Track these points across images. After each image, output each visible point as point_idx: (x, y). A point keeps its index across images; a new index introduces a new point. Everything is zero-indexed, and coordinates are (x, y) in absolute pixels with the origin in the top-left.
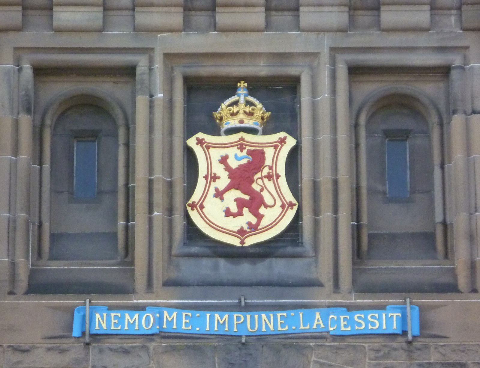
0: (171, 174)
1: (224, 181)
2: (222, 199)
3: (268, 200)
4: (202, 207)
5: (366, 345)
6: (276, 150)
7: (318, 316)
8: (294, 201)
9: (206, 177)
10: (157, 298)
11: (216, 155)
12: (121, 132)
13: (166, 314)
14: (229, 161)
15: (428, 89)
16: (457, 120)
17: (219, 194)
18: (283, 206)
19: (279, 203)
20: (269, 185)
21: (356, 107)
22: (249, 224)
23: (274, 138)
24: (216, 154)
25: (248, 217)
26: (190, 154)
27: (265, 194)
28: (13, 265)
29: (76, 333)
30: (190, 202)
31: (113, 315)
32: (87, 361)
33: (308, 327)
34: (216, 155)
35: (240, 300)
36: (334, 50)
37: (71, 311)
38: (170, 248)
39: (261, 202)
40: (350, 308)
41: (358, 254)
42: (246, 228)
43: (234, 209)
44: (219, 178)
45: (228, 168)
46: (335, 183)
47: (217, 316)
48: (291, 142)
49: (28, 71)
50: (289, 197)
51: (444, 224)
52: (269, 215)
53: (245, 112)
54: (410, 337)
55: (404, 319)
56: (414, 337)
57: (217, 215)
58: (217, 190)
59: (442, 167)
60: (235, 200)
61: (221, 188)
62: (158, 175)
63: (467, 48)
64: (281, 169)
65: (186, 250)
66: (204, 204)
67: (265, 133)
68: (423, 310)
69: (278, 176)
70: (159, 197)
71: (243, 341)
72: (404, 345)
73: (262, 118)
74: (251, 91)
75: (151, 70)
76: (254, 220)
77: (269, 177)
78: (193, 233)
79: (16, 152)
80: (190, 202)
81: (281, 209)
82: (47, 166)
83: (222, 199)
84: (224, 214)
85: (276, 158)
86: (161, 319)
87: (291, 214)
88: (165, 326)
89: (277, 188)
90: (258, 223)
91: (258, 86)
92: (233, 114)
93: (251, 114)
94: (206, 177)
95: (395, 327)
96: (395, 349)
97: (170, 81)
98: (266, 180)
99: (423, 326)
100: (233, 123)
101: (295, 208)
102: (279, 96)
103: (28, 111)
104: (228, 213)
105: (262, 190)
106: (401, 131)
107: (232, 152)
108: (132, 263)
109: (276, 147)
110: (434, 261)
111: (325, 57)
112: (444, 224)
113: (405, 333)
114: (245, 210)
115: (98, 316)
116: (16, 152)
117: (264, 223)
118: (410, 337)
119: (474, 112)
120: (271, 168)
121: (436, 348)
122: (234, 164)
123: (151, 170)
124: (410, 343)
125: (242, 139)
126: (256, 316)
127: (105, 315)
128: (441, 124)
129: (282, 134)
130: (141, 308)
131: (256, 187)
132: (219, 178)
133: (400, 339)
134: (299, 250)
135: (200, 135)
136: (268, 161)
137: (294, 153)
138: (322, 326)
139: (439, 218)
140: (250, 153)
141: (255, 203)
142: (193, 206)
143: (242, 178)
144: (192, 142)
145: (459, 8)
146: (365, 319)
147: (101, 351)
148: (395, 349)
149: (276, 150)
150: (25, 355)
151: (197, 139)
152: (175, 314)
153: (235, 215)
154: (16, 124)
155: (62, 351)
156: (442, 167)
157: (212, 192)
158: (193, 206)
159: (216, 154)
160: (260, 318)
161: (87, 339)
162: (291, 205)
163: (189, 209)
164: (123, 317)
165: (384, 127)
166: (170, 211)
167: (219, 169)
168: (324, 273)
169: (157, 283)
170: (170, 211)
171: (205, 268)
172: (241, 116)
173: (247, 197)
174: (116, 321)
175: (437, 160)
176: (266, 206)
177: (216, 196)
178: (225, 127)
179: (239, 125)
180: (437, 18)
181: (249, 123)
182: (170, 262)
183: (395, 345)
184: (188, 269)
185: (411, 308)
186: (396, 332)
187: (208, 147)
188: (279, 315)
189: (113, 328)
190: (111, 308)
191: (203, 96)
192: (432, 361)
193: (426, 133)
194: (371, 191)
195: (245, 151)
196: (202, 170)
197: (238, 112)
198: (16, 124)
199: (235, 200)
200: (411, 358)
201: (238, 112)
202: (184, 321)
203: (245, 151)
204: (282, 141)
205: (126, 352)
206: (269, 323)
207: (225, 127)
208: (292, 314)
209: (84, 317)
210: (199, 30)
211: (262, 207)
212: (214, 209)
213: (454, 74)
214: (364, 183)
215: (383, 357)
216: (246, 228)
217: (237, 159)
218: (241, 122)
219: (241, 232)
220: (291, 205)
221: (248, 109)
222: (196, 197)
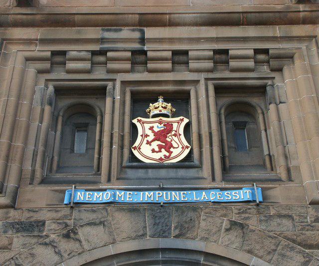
0: (123, 131)
1: (152, 137)
2: (150, 145)
3: (175, 145)
4: (140, 148)
5: (232, 207)
6: (179, 124)
7: (204, 193)
8: (189, 145)
9: (142, 136)
10: (113, 185)
11: (147, 127)
12: (99, 118)
13: (118, 193)
14: (154, 129)
15: (255, 101)
16: (272, 107)
17: (149, 143)
18: (183, 148)
19: (181, 146)
20: (176, 139)
21: (219, 108)
22: (165, 156)
23: (178, 119)
24: (147, 126)
25: (164, 152)
26: (134, 128)
27: (173, 143)
28: (33, 171)
29: (66, 202)
30: (134, 146)
31: (87, 193)
32: (71, 216)
33: (199, 199)
34: (147, 127)
35: (160, 186)
36: (207, 79)
37: (63, 192)
38: (122, 163)
39: (172, 146)
40: (222, 189)
41: (224, 169)
42: (163, 157)
43: (157, 149)
44: (149, 136)
45: (153, 132)
46: (210, 134)
47: (147, 193)
48: (186, 121)
49: (51, 88)
50: (186, 143)
51: (269, 155)
52: (175, 152)
53: (162, 107)
54: (258, 202)
55: (253, 194)
56: (260, 202)
57: (147, 152)
58: (148, 141)
59: (266, 131)
60: (157, 146)
61: (150, 140)
62: (116, 129)
63: (274, 78)
64: (181, 131)
65: (131, 164)
66: (141, 147)
67: (172, 117)
68: (263, 190)
69: (180, 135)
70: (116, 139)
71: (162, 204)
72: (255, 207)
73: (171, 110)
74: (165, 100)
75: (114, 88)
76: (167, 154)
77: (175, 135)
78: (133, 158)
79: (41, 122)
80: (134, 146)
81: (182, 149)
82: (59, 133)
83: (150, 145)
84: (151, 151)
85: (178, 127)
86: (114, 195)
87: (187, 151)
88: (117, 199)
89: (180, 140)
90: (170, 155)
91: (168, 97)
92: (156, 108)
93: (165, 108)
94: (142, 136)
95: (248, 197)
96: (250, 209)
97: (123, 94)
98: (173, 137)
99: (265, 198)
100: (157, 112)
101: (189, 149)
102: (180, 100)
103: (50, 104)
104: (153, 151)
105: (171, 141)
106: (242, 122)
107: (155, 125)
108: (100, 174)
109: (178, 123)
110: (266, 172)
111: (202, 82)
112: (269, 155)
113: (255, 201)
114: (163, 150)
115: (79, 193)
116: (41, 122)
117: (172, 155)
118: (258, 202)
119: (281, 103)
120: (176, 131)
121: (273, 208)
122: (156, 130)
123: (112, 128)
124: (258, 205)
125: (161, 119)
126: (169, 193)
127: (83, 193)
128: (263, 113)
129: (182, 117)
130: (105, 190)
131: (168, 139)
132: (149, 136)
133: (252, 204)
134: (192, 163)
135: (139, 118)
136: (175, 128)
137: (188, 127)
138: (207, 198)
139: (266, 152)
140: (164, 125)
141: (168, 147)
142: (135, 148)
143: (161, 136)
144: (135, 121)
145: (268, 62)
146: (231, 194)
147: (79, 211)
148: (250, 209)
149: (179, 124)
150: (35, 213)
151: (138, 120)
152: (123, 193)
153: (157, 152)
154: (43, 111)
155: (57, 211)
156: (266, 131)
157: (145, 142)
158: (135, 148)
159: (147, 126)
160: (171, 194)
161: (72, 205)
162: (187, 147)
163: (133, 150)
164: (93, 195)
165: (233, 120)
166: (122, 147)
167: (149, 132)
168: (206, 172)
169: (113, 179)
170: (122, 147)
171: (141, 173)
172: (160, 108)
173: (164, 144)
174: (89, 196)
175: (262, 128)
176: (174, 148)
177: (147, 144)
178: (152, 114)
179: (159, 113)
180: (258, 67)
181: (164, 111)
182: (121, 170)
183: (249, 207)
184: (131, 173)
185: (257, 189)
186: (249, 199)
187: (143, 123)
188: (182, 192)
189: (87, 199)
190: (87, 190)
191: (141, 101)
192: (271, 214)
193: (255, 121)
194: (229, 147)
195: (162, 125)
196: (140, 132)
197: (159, 107)
198: (43, 111)
199: (157, 146)
200: (259, 213)
201: (159, 107)
202: (128, 196)
203: (162, 125)
204: (182, 120)
205: (94, 211)
206: (176, 196)
207: (152, 114)
208: (189, 193)
209: (71, 195)
210: (138, 72)
211: (172, 148)
212: (146, 150)
213: (268, 88)
214: (225, 137)
215: (243, 213)
216: (163, 157)
217: (157, 128)
218: (160, 111)
219: (161, 159)
220: (187, 147)
221: (163, 106)
222: (136, 144)
